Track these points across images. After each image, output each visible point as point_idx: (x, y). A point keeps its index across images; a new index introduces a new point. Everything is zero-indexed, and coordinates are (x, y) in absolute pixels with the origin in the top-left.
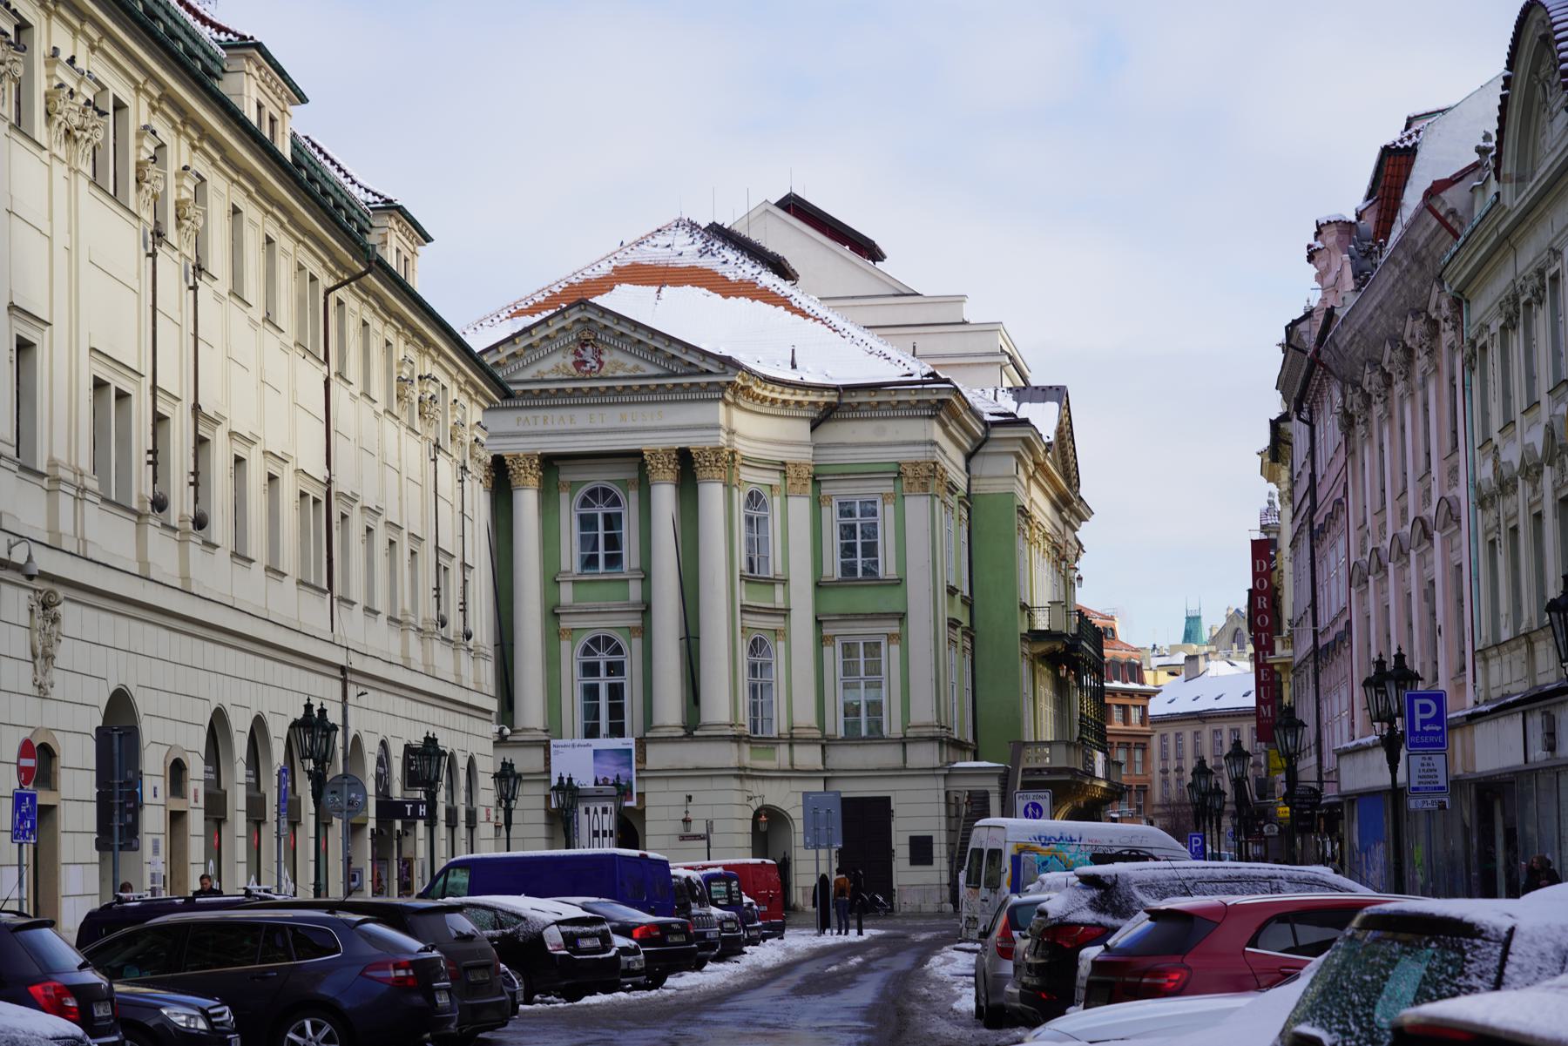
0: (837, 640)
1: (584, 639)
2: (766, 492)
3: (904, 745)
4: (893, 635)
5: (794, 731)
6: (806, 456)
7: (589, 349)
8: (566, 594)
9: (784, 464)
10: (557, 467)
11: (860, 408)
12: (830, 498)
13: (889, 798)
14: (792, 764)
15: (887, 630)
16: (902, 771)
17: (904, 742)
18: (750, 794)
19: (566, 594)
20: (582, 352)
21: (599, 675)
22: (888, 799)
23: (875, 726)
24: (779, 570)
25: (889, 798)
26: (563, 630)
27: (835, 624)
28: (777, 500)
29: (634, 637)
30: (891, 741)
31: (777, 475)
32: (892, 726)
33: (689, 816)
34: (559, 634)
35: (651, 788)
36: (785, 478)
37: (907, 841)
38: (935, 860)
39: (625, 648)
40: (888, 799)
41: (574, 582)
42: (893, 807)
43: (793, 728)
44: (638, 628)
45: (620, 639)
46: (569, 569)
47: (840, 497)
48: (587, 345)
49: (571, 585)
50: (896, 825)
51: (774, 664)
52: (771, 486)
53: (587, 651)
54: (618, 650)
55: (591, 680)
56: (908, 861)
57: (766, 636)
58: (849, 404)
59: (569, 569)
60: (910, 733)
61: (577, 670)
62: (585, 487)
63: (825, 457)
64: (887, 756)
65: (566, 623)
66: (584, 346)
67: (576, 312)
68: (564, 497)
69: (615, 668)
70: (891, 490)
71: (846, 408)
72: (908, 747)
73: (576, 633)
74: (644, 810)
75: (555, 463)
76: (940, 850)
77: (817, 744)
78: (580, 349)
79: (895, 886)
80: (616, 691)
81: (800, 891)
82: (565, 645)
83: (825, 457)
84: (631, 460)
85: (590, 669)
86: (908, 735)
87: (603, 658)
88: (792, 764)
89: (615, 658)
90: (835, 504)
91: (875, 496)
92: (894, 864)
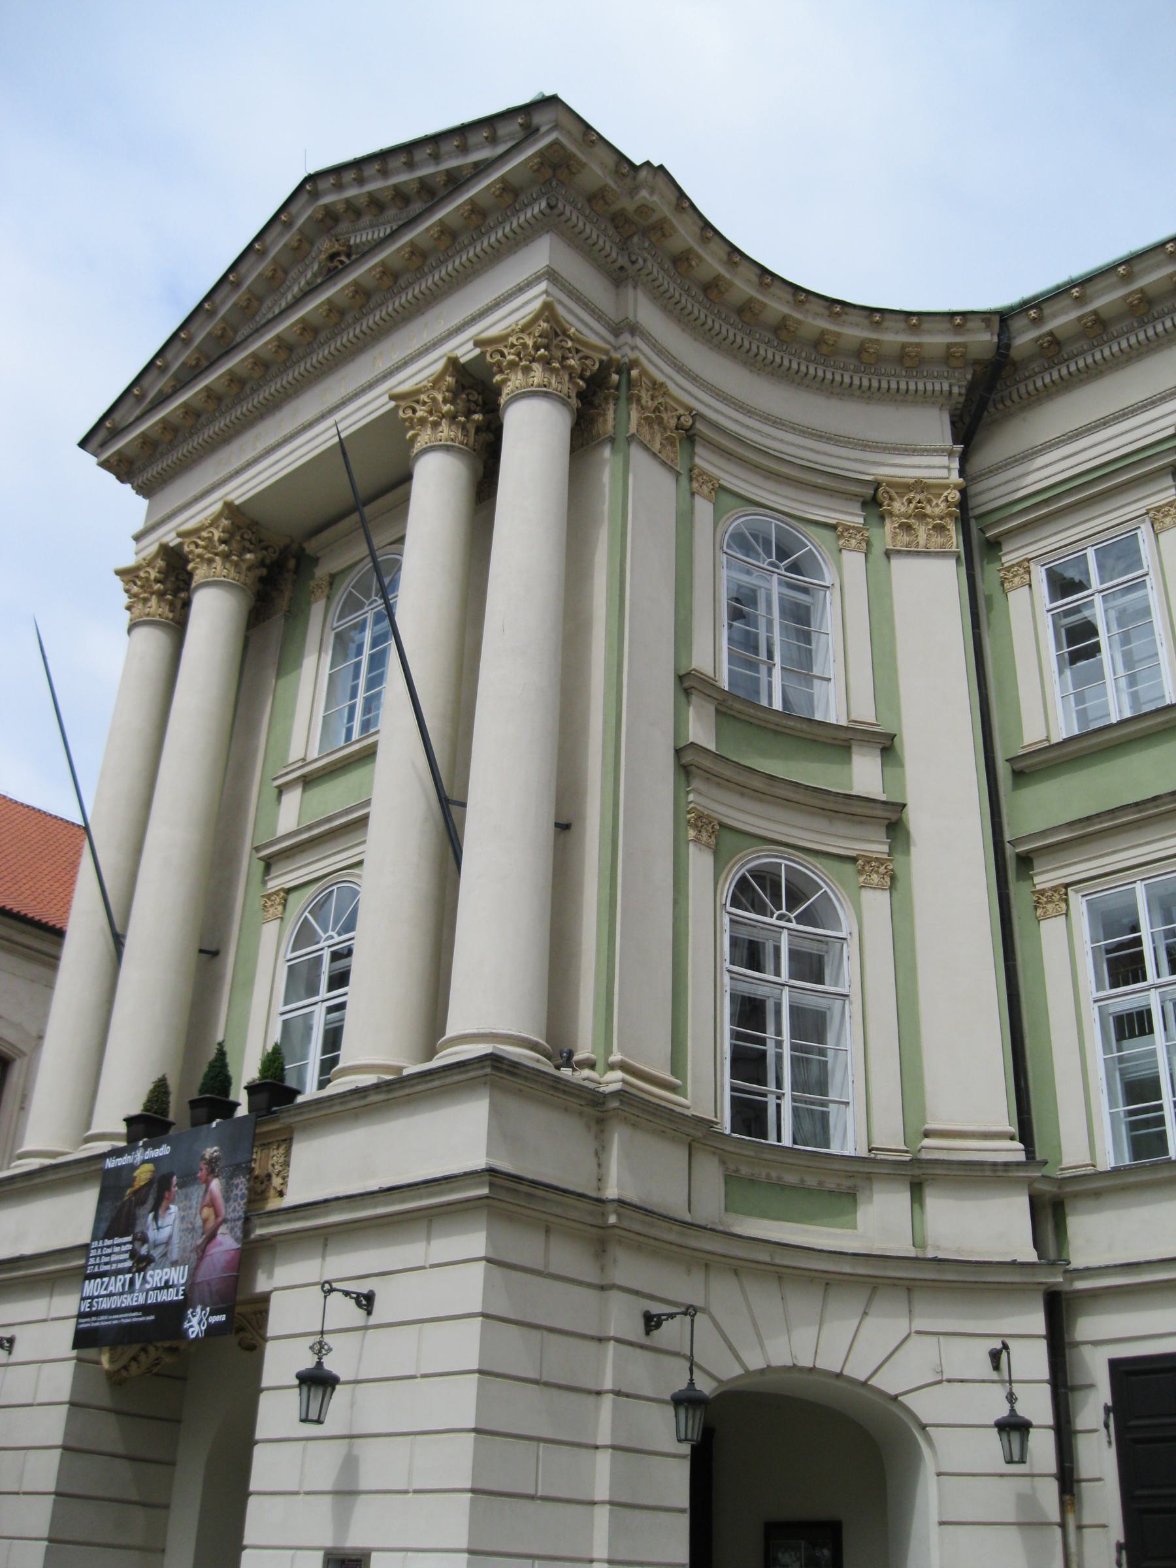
2: (815, 543)
5: (927, 1142)
6: (944, 473)
9: (877, 485)
12: (1024, 566)
14: (918, 1241)
18: (657, 1308)
24: (865, 712)
28: (853, 562)
31: (856, 508)
33: (330, 1364)
43: (927, 1134)
51: (850, 950)
52: (833, 527)
57: (814, 870)
62: (353, 574)
67: (304, 208)
68: (317, 610)
71: (1035, 366)
73: (292, 897)
77: (1014, 1183)
82: (270, 931)
88: (918, 1241)
90: (1039, 576)
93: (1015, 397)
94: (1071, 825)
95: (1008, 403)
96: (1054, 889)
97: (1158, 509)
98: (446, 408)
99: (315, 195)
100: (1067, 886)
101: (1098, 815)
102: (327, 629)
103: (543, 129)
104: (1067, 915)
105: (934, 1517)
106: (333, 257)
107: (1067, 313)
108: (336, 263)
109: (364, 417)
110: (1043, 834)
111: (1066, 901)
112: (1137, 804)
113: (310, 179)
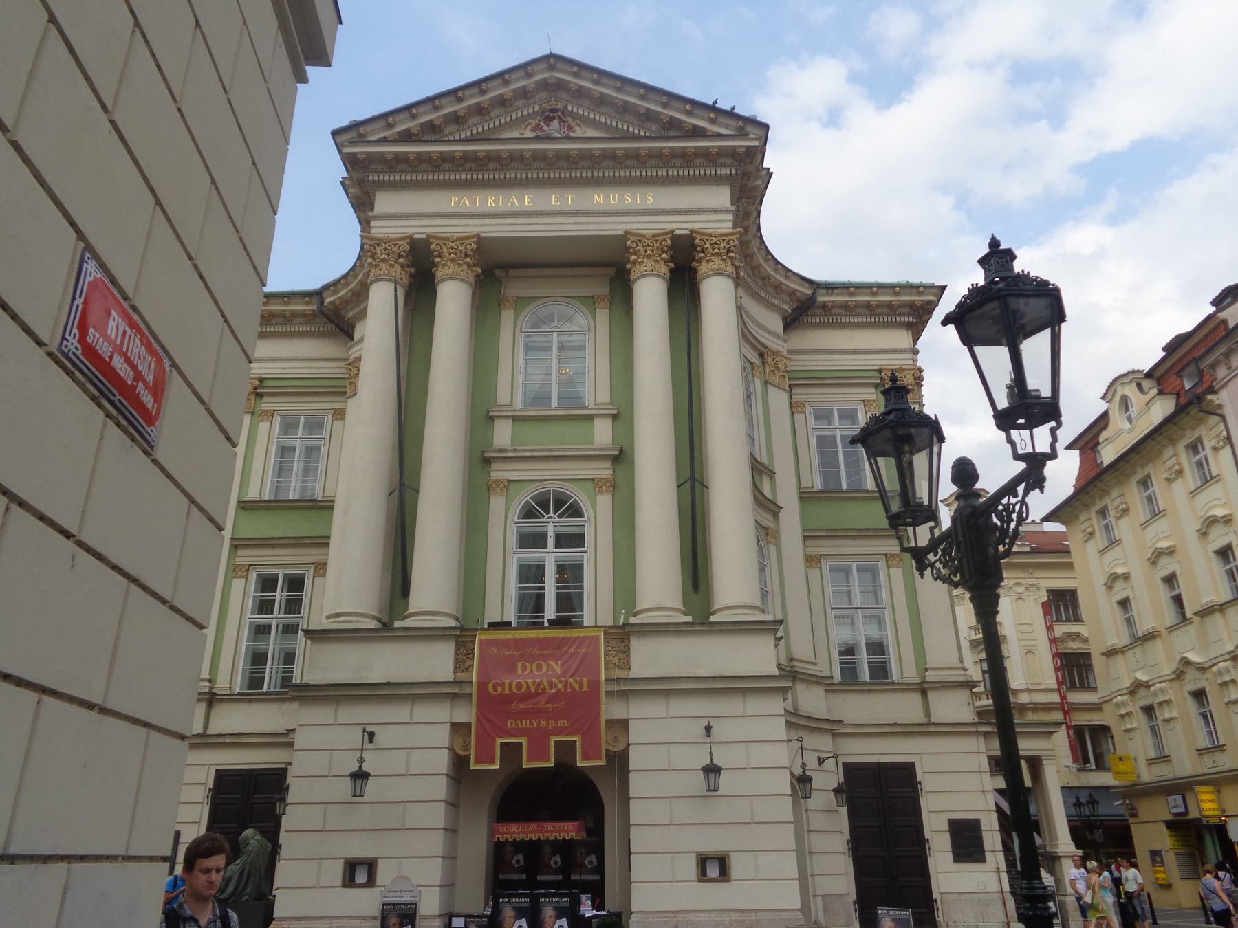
0: (823, 563)
1: (525, 496)
3: (924, 692)
4: (893, 555)
7: (555, 122)
8: (502, 435)
10: (500, 281)
11: (834, 311)
13: (913, 764)
15: (885, 550)
16: (926, 729)
17: (923, 689)
19: (502, 435)
20: (545, 128)
21: (546, 547)
22: (909, 768)
23: (880, 671)
25: (913, 764)
26: (495, 481)
27: (819, 542)
29: (601, 493)
30: (905, 687)
32: (902, 667)
34: (490, 487)
35: (635, 710)
36: (763, 363)
37: (946, 827)
38: (988, 855)
39: (586, 507)
40: (909, 768)
41: (515, 419)
42: (919, 778)
44: (607, 480)
45: (579, 496)
46: (509, 402)
47: (812, 404)
48: (555, 118)
49: (510, 422)
50: (928, 804)
53: (529, 513)
54: (576, 512)
55: (532, 555)
56: (950, 856)
58: (824, 306)
59: (509, 402)
60: (931, 676)
61: (513, 540)
63: (798, 363)
64: (907, 708)
65: (499, 472)
66: (548, 120)
69: (574, 540)
70: (873, 397)
71: (818, 312)
72: (931, 694)
73: (513, 486)
74: (626, 749)
75: (498, 273)
76: (992, 839)
78: (542, 124)
79: (936, 895)
80: (570, 573)
81: (819, 900)
82: (497, 504)
83: (798, 363)
84: (601, 270)
85: (533, 540)
86: (928, 679)
87: (551, 525)
89: (568, 525)
90: (809, 410)
91: (856, 403)
92: (930, 860)
93: (805, 321)
94: (827, 530)
95: (801, 323)
96: (815, 556)
97: (869, 401)
98: (664, 255)
99: (552, 68)
100: (821, 555)
101: (840, 529)
102: (517, 331)
103: (751, 136)
104: (820, 568)
105: (806, 831)
106: (553, 111)
107: (843, 296)
108: (555, 115)
109: (595, 230)
110: (814, 530)
111: (820, 562)
112: (858, 529)
113: (552, 55)
